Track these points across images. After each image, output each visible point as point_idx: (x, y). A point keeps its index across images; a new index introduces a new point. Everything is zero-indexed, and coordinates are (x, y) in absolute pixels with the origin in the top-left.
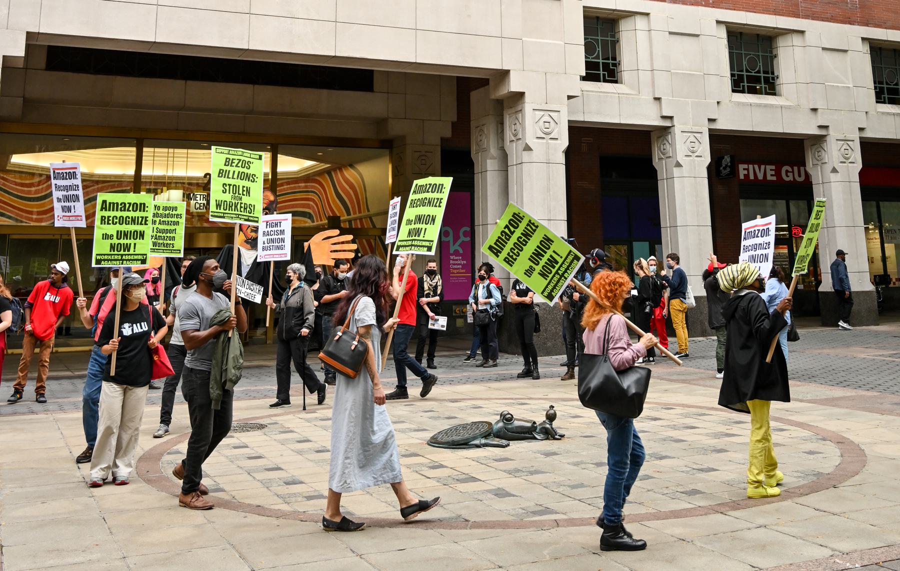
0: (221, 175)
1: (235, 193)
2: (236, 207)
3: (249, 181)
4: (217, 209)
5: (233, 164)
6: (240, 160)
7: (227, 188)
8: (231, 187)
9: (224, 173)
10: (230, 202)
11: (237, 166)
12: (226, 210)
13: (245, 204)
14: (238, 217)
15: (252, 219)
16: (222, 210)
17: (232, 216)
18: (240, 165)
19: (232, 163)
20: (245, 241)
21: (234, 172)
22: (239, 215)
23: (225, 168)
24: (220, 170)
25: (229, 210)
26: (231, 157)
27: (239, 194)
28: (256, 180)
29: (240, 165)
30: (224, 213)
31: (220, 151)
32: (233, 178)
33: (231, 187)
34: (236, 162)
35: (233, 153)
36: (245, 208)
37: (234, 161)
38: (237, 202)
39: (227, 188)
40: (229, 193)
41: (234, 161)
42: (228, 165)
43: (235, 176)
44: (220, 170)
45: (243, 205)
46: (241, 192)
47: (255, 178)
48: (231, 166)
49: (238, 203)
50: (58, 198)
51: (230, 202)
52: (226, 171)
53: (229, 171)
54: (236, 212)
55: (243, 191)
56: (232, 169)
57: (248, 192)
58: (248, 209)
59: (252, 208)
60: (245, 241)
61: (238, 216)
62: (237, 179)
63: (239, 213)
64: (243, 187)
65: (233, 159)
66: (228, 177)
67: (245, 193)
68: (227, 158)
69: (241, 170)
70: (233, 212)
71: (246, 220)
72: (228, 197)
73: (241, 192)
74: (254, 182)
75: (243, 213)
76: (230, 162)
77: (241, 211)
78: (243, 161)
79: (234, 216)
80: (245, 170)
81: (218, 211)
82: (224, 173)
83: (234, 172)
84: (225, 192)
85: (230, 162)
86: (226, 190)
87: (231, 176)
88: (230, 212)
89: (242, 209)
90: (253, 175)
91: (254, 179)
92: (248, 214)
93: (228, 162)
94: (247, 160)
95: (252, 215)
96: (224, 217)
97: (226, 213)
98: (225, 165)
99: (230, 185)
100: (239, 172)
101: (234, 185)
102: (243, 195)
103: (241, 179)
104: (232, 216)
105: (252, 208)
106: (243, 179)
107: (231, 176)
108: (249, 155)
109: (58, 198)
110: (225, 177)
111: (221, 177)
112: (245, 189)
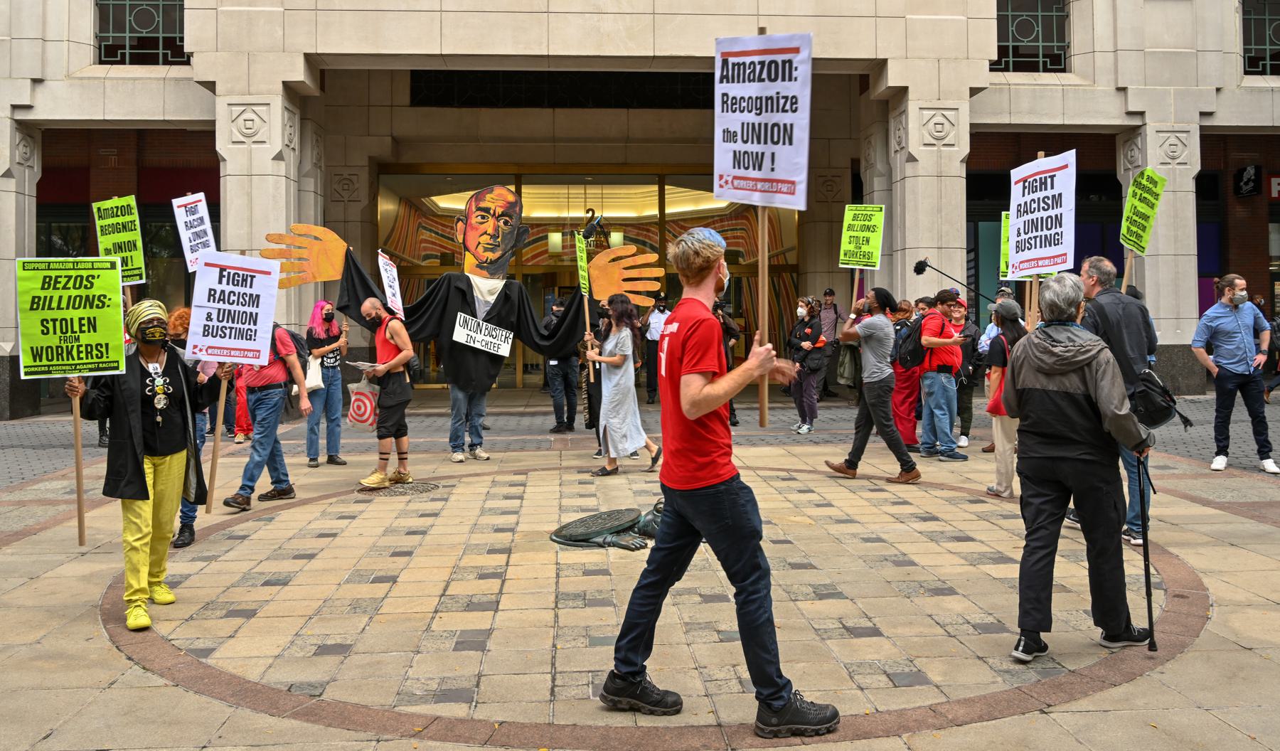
0: (35, 306)
1: (67, 332)
2: (69, 353)
4: (35, 361)
5: (58, 286)
6: (70, 277)
7: (50, 325)
8: (58, 324)
9: (41, 303)
10: (57, 347)
11: (65, 288)
12: (52, 360)
13: (87, 346)
14: (75, 369)
15: (104, 365)
16: (45, 362)
17: (64, 368)
18: (71, 284)
19: (56, 282)
20: (478, 266)
21: (61, 298)
22: (76, 365)
23: (42, 294)
24: (34, 298)
25: (58, 360)
27: (73, 332)
29: (71, 284)
30: (49, 366)
31: (32, 266)
32: (59, 308)
33: (58, 324)
34: (63, 281)
35: (56, 266)
36: (87, 353)
37: (59, 280)
38: (70, 345)
39: (50, 325)
40: (55, 333)
41: (59, 280)
43: (64, 304)
44: (34, 298)
46: (76, 328)
47: (106, 300)
48: (55, 288)
49: (73, 347)
50: (726, 131)
51: (57, 347)
52: (46, 297)
53: (51, 297)
54: (71, 362)
55: (81, 325)
56: (56, 294)
57: (92, 325)
58: (95, 352)
59: (103, 350)
60: (478, 266)
61: (75, 368)
62: (68, 308)
63: (77, 362)
64: (81, 319)
65: (57, 277)
66: (50, 308)
67: (85, 328)
69: (74, 293)
70: (66, 362)
71: (91, 370)
72: (53, 340)
73: (76, 328)
74: (103, 306)
75: (85, 361)
76: (52, 282)
77: (79, 358)
79: (67, 368)
80: (83, 292)
81: (38, 363)
82: (41, 303)
83: (61, 298)
84: (48, 333)
85: (52, 282)
86: (48, 329)
87: (54, 305)
88: (60, 362)
89: (83, 355)
90: (100, 296)
91: (104, 303)
92: (95, 360)
93: (47, 283)
94: (85, 273)
95: (104, 359)
96: (49, 372)
97: (52, 366)
98: (43, 288)
99: (54, 321)
100: (70, 297)
101: (62, 320)
102: (82, 331)
104: (64, 368)
105: (103, 350)
106: (79, 307)
107: (54, 305)
108: (90, 266)
109: (726, 131)
110: (43, 309)
111: (37, 309)
112: (85, 322)
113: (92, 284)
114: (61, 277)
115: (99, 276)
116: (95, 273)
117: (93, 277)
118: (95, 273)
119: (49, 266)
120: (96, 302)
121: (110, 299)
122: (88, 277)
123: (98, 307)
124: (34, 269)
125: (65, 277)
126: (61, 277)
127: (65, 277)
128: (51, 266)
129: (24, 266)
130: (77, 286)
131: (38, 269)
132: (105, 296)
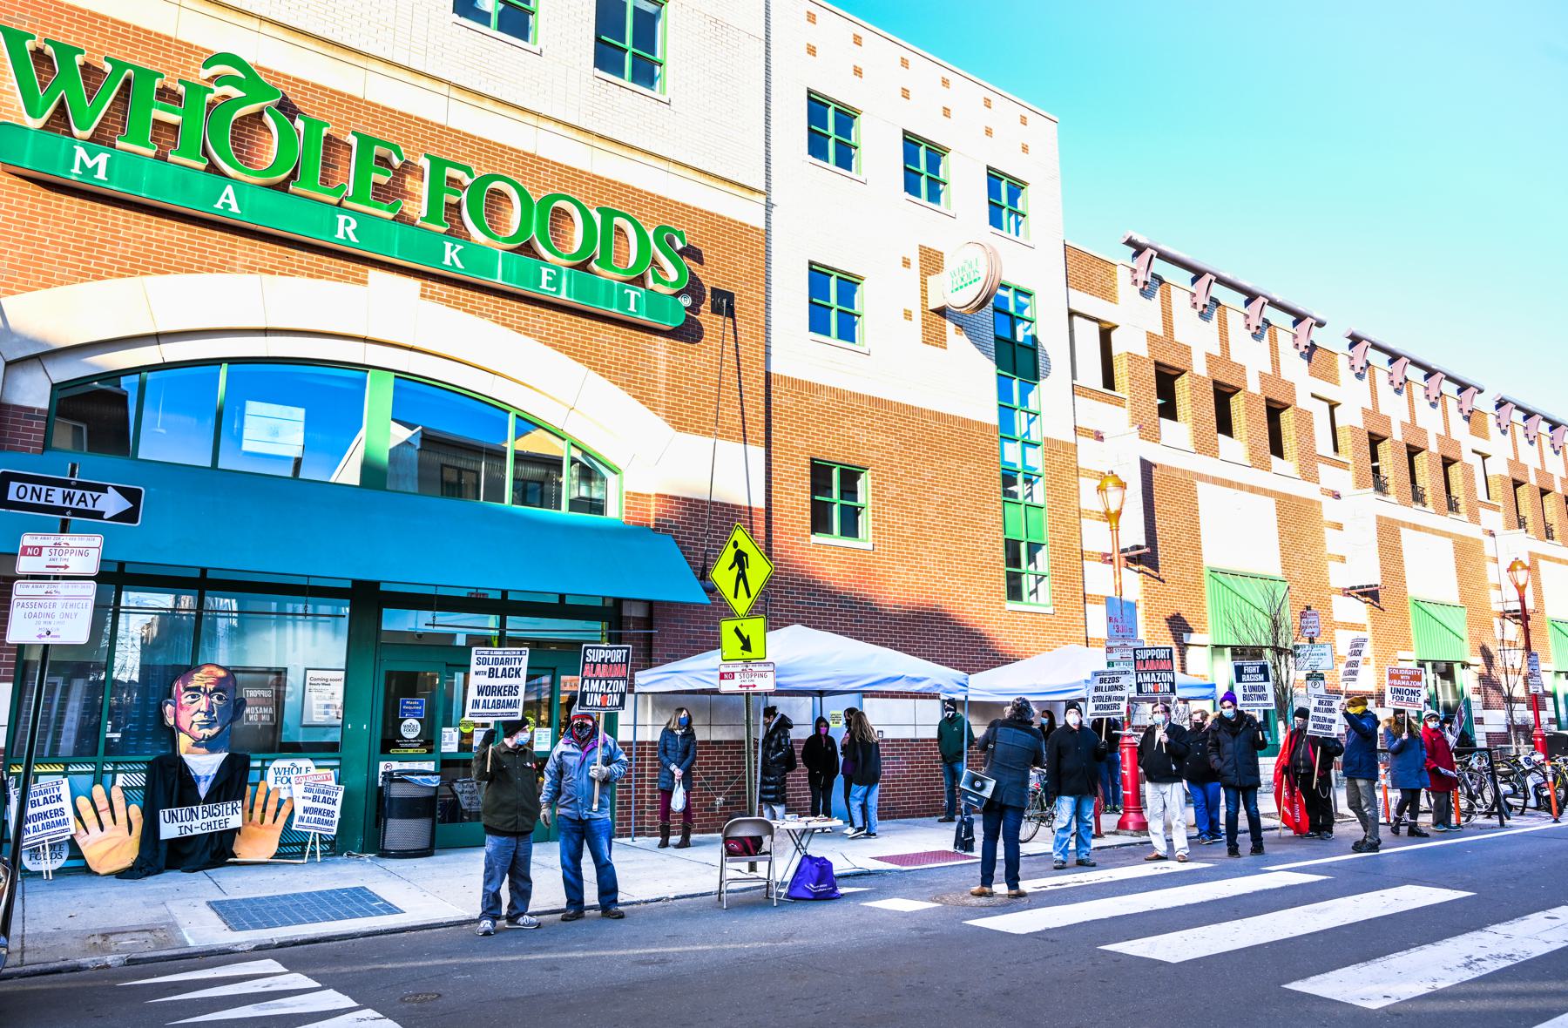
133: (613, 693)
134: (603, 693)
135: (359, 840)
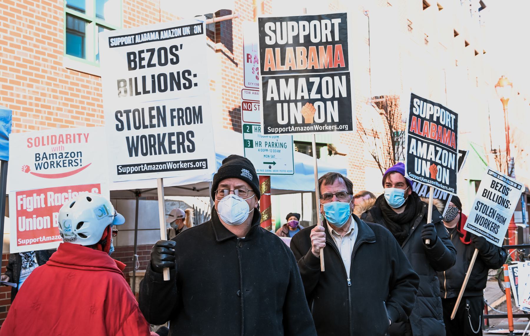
3: (179, 88)
6: (152, 51)
11: (150, 65)
18: (155, 60)
21: (144, 78)
26: (136, 49)
28: (194, 80)
29: (155, 60)
36: (179, 144)
37: (143, 55)
41: (143, 55)
42: (135, 68)
43: (149, 87)
45: (174, 138)
47: (191, 77)
68: (129, 54)
69: (158, 70)
74: (190, 86)
76: (137, 60)
78: (160, 50)
80: (168, 69)
83: (144, 78)
85: (137, 60)
89: (174, 147)
90: (184, 73)
91: (190, 81)
94: (167, 44)
98: (130, 68)
103: (160, 90)
106: (166, 89)
113: (177, 56)
114: (143, 51)
115: (181, 45)
116: (176, 42)
117: (176, 47)
118: (176, 42)
119: (135, 38)
120: (183, 81)
121: (195, 76)
122: (171, 48)
123: (185, 87)
124: (120, 45)
125: (148, 51)
126: (143, 51)
127: (148, 51)
128: (138, 40)
129: (110, 43)
130: (163, 61)
131: (124, 45)
132: (189, 73)
133: (443, 166)
134: (432, 162)
135: (173, 270)
